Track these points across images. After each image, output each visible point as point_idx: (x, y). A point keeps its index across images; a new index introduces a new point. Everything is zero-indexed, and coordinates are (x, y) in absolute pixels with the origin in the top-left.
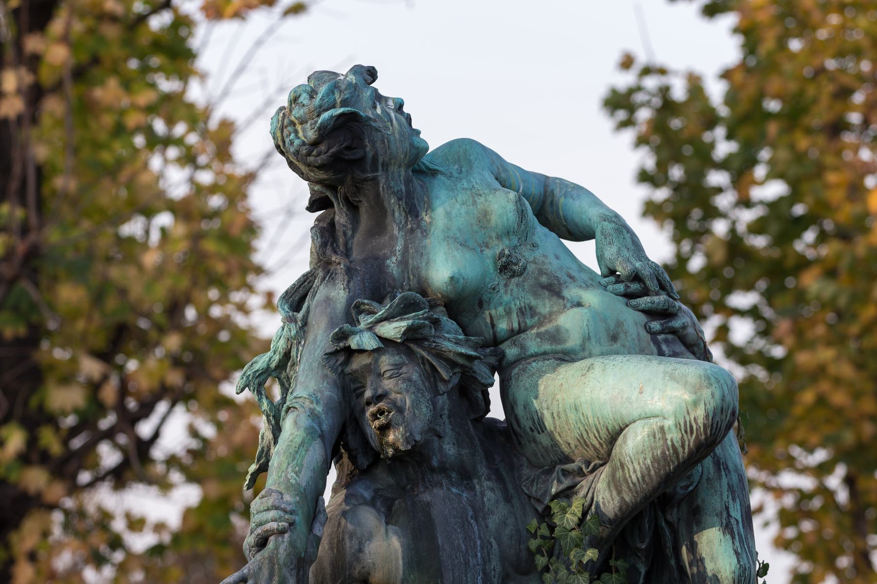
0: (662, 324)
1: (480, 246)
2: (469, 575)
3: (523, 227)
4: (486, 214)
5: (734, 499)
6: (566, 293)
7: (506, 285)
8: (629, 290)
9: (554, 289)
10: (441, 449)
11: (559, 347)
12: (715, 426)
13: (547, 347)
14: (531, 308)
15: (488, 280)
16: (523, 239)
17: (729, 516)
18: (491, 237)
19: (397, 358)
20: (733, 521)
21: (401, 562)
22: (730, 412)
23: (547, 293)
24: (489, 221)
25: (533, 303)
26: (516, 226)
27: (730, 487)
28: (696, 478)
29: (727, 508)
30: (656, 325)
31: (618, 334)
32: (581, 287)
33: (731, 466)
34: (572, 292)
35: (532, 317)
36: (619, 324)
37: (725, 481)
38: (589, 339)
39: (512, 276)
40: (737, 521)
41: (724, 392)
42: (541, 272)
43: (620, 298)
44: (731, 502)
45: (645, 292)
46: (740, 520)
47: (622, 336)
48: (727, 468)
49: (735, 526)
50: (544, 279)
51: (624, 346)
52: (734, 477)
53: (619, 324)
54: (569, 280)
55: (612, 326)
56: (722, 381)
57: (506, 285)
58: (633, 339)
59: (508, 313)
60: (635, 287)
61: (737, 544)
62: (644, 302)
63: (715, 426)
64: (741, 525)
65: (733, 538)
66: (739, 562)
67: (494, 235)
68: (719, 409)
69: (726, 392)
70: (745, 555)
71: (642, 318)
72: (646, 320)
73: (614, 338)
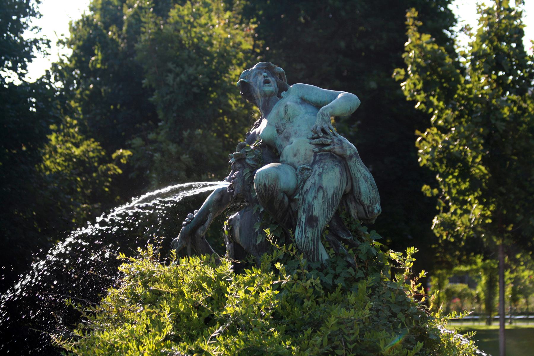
5: (304, 214)
6: (291, 139)
9: (287, 138)
27: (304, 210)
30: (317, 150)
32: (296, 137)
33: (307, 202)
36: (298, 150)
42: (286, 132)
45: (319, 137)
47: (298, 155)
48: (305, 203)
50: (286, 135)
52: (306, 206)
53: (298, 150)
60: (315, 136)
62: (314, 141)
69: (261, 178)
71: (313, 146)
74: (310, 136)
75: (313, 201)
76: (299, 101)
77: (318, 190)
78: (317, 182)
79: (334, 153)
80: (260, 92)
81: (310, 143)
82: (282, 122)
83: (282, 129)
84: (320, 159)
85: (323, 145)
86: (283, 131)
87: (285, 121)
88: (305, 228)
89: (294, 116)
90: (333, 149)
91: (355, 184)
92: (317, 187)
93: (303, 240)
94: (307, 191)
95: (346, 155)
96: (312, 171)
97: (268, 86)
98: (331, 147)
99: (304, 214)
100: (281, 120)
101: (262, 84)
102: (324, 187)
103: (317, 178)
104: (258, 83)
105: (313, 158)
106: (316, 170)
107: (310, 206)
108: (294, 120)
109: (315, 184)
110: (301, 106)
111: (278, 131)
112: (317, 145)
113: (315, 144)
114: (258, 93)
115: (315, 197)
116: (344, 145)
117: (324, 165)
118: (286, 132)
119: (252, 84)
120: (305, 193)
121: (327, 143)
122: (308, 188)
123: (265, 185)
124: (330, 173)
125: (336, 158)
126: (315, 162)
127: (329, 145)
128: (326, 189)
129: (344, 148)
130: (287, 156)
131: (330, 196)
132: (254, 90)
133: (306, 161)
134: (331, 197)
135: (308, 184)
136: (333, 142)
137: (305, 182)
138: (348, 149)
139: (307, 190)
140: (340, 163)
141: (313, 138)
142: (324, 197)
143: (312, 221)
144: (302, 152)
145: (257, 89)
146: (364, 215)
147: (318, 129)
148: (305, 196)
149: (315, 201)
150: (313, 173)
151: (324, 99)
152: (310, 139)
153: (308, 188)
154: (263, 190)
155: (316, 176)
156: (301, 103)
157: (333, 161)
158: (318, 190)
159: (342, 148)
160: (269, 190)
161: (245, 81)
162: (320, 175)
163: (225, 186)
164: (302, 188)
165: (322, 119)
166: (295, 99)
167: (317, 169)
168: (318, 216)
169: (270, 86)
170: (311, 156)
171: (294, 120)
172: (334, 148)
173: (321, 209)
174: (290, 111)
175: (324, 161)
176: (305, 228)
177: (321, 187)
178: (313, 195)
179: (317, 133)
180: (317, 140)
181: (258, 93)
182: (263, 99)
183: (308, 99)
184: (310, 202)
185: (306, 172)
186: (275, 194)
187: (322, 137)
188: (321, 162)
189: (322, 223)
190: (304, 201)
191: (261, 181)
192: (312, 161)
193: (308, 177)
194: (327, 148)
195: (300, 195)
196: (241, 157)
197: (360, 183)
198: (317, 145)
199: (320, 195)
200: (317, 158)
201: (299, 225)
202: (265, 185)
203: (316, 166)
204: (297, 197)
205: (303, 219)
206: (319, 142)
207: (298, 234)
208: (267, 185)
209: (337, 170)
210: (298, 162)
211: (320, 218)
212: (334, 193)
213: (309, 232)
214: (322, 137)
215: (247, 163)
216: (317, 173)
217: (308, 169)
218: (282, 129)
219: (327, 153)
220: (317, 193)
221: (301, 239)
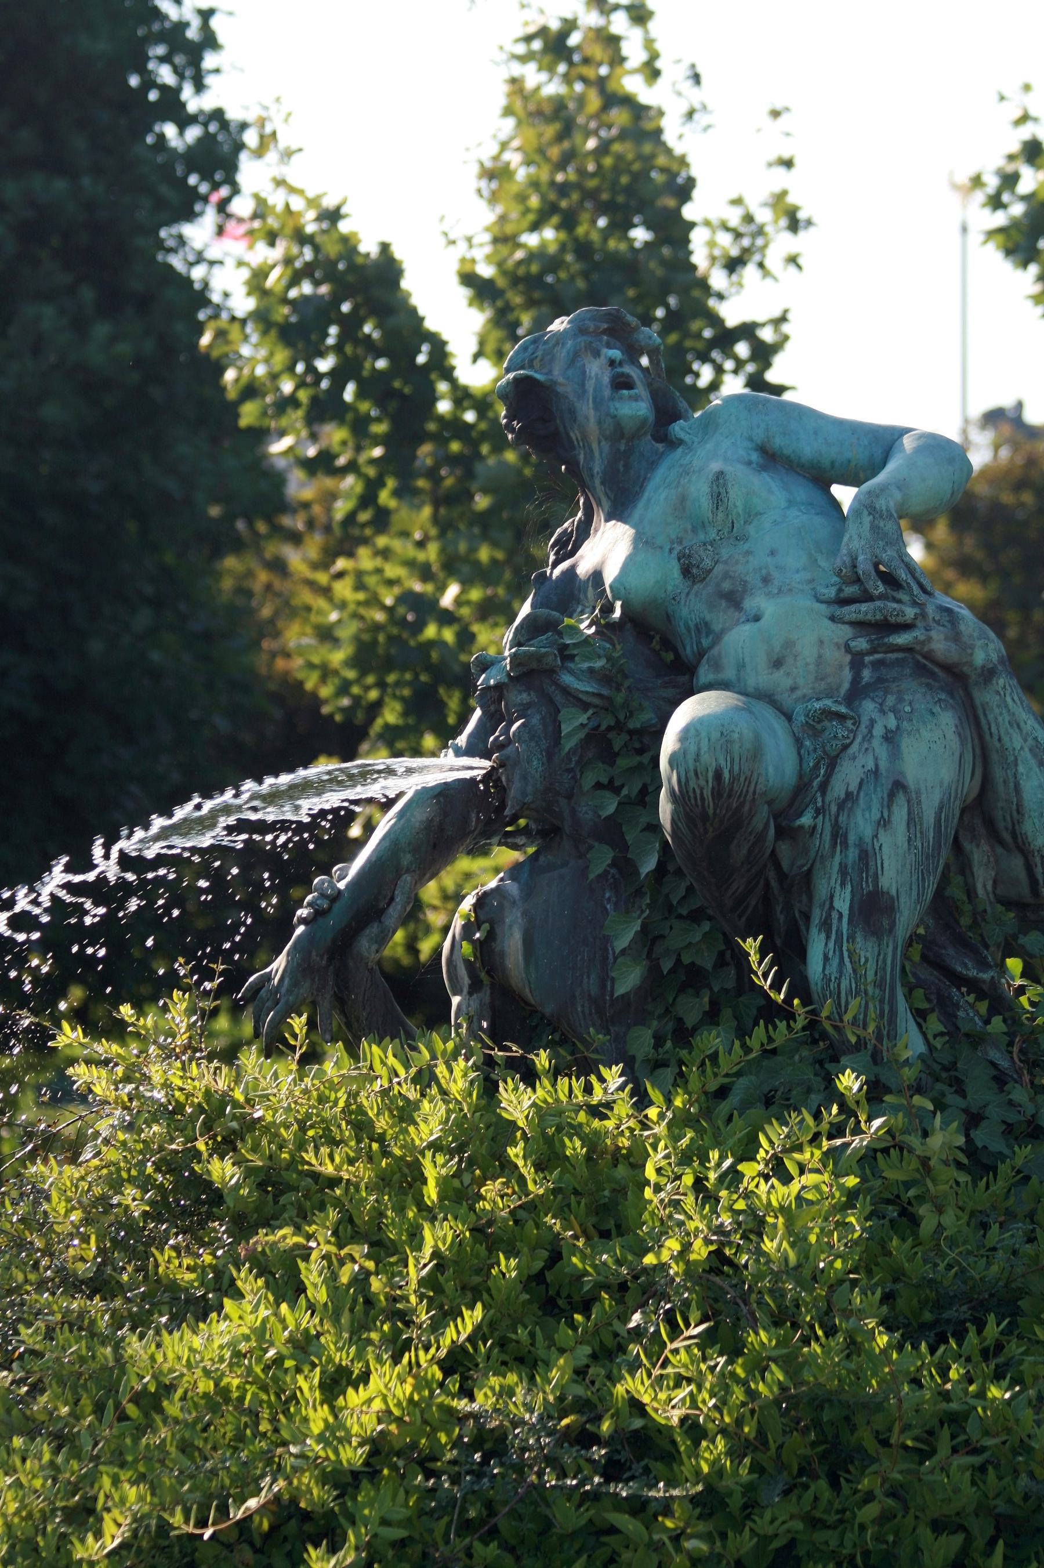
0: (871, 641)
1: (672, 542)
2: (592, 976)
3: (721, 516)
4: (683, 499)
5: (843, 885)
6: (750, 604)
7: (688, 594)
8: (842, 595)
9: (733, 599)
10: (573, 812)
11: (721, 676)
12: (691, 794)
13: (711, 677)
14: (706, 624)
15: (670, 588)
16: (726, 531)
17: (832, 907)
18: (686, 531)
19: (524, 696)
20: (835, 915)
21: (520, 958)
22: (710, 775)
23: (724, 603)
24: (684, 509)
25: (708, 618)
26: (710, 515)
27: (843, 871)
28: (812, 854)
29: (832, 897)
30: (861, 644)
31: (784, 657)
32: (768, 595)
33: (852, 838)
34: (755, 602)
35: (707, 636)
36: (789, 644)
37: (838, 858)
38: (744, 666)
39: (694, 583)
40: (841, 915)
41: (699, 749)
42: (726, 575)
43: (823, 607)
44: (838, 888)
45: (867, 597)
46: (846, 913)
47: (790, 660)
48: (845, 844)
49: (835, 922)
50: (726, 586)
51: (788, 674)
52: (852, 854)
53: (789, 644)
54: (760, 584)
55: (777, 649)
56: (703, 734)
57: (688, 594)
58: (808, 664)
59: (689, 630)
60: (850, 591)
61: (831, 945)
63: (691, 794)
64: (845, 920)
65: (828, 937)
66: (824, 969)
67: (689, 527)
68: (692, 774)
70: (837, 960)
71: (846, 631)
72: (850, 635)
73: (777, 664)
74: (831, 593)
75: (876, 836)
76: (755, 456)
77: (892, 795)
78: (883, 765)
79: (929, 656)
80: (599, 423)
81: (832, 619)
82: (702, 536)
83: (708, 562)
84: (880, 680)
85: (887, 626)
86: (711, 570)
87: (713, 534)
88: (851, 938)
89: (751, 515)
90: (922, 643)
91: (998, 773)
92: (887, 783)
93: (844, 984)
94: (849, 799)
95: (970, 664)
96: (857, 723)
97: (630, 397)
98: (918, 633)
99: (843, 885)
100: (694, 530)
101: (607, 392)
102: (912, 785)
103: (881, 750)
104: (590, 386)
105: (847, 675)
106: (872, 722)
107: (866, 856)
108: (751, 529)
109: (876, 772)
110: (765, 474)
111: (686, 571)
112: (860, 625)
113: (852, 623)
114: (592, 427)
115: (884, 823)
116: (962, 627)
117: (900, 700)
118: (726, 575)
119: (566, 388)
120: (841, 807)
121: (900, 620)
122: (853, 787)
123: (718, 775)
124: (924, 732)
125: (932, 675)
126: (856, 693)
127: (907, 627)
128: (918, 793)
129: (965, 639)
130: (741, 666)
131: (929, 817)
132: (573, 412)
133: (823, 685)
134: (932, 820)
135: (849, 775)
136: (923, 615)
137: (833, 763)
138: (979, 643)
139: (849, 795)
140: (951, 694)
141: (843, 602)
142: (911, 821)
143: (873, 910)
144: (807, 650)
145: (587, 411)
146: (1026, 890)
147: (864, 565)
148: (842, 819)
149: (884, 838)
150: (863, 729)
151: (848, 455)
152: (828, 602)
153: (853, 787)
154: (708, 793)
155: (876, 742)
156: (763, 468)
157: (929, 686)
158: (892, 795)
159: (956, 637)
160: (729, 796)
161: (537, 376)
162: (891, 738)
163: (467, 775)
164: (824, 787)
165: (874, 528)
166: (741, 452)
167: (875, 715)
168: (893, 892)
169: (636, 398)
170: (841, 667)
171: (751, 529)
172: (930, 639)
173: (904, 866)
174: (736, 496)
175: (894, 686)
176: (851, 938)
177: (899, 786)
178: (876, 815)
179: (858, 580)
180: (864, 607)
181: (592, 427)
182: (606, 446)
183: (787, 451)
184: (868, 839)
185: (833, 727)
186: (747, 808)
187: (882, 597)
188: (887, 692)
189: (908, 916)
190: (839, 836)
191: (706, 758)
192: (846, 686)
193: (845, 747)
194: (902, 639)
195: (818, 812)
196: (534, 665)
197: (1021, 769)
198: (860, 625)
199: (900, 813)
200: (867, 674)
201: (826, 926)
202: (718, 775)
203: (868, 707)
204: (806, 820)
205: (843, 903)
206: (869, 617)
207: (826, 958)
208: (726, 775)
209: (948, 720)
210: (793, 689)
211: (902, 900)
212: (941, 809)
213: (866, 949)
214: (882, 597)
215: (566, 691)
216: (878, 731)
217: (841, 717)
218: (708, 562)
219: (900, 655)
220: (889, 807)
221: (839, 980)
